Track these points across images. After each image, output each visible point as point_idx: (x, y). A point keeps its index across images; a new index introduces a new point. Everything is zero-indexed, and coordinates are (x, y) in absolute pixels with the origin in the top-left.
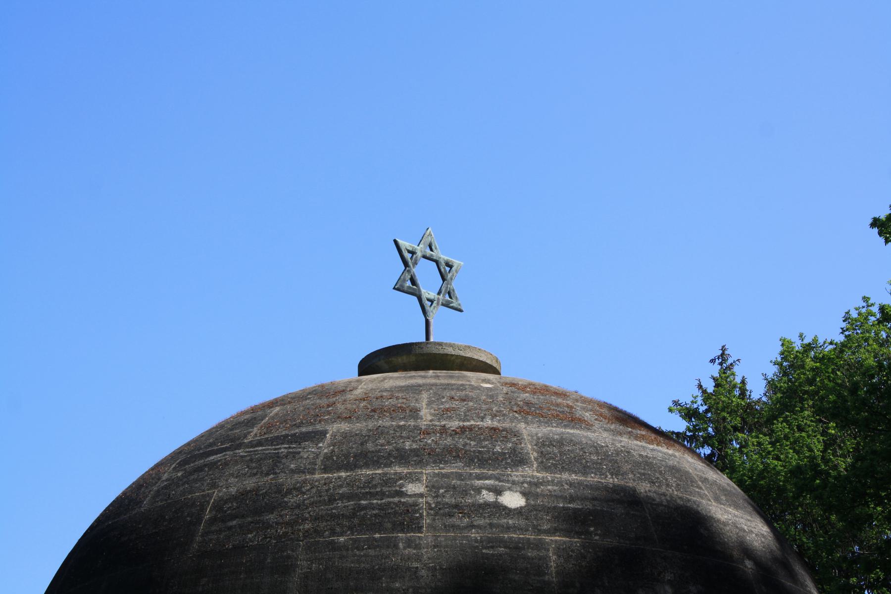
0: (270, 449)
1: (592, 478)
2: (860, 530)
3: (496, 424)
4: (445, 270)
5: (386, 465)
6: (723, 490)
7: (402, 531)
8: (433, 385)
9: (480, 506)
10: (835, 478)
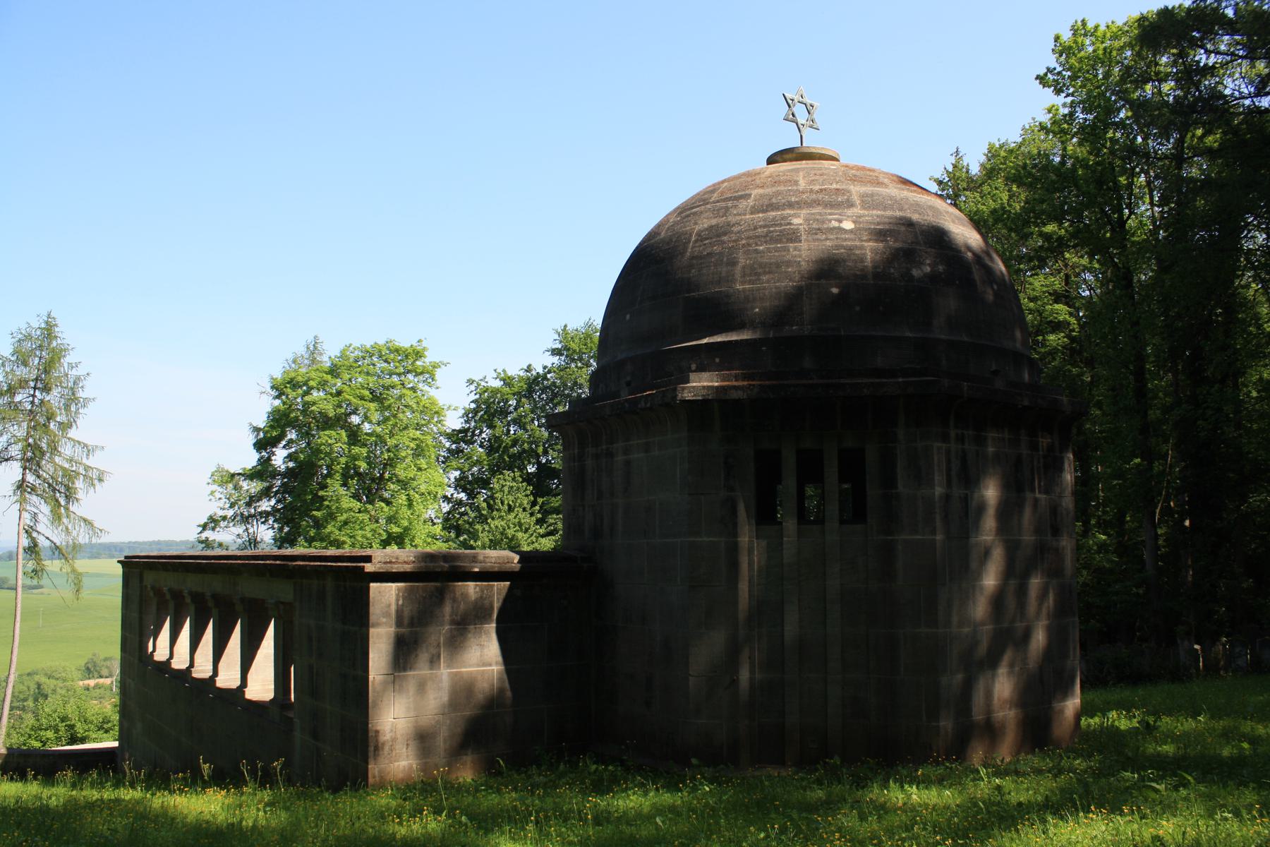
0: (723, 204)
1: (889, 213)
2: (1026, 240)
3: (838, 187)
4: (809, 109)
5: (782, 210)
6: (956, 217)
7: (792, 243)
8: (804, 168)
9: (831, 229)
10: (1014, 214)
